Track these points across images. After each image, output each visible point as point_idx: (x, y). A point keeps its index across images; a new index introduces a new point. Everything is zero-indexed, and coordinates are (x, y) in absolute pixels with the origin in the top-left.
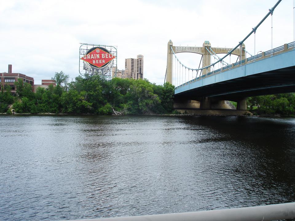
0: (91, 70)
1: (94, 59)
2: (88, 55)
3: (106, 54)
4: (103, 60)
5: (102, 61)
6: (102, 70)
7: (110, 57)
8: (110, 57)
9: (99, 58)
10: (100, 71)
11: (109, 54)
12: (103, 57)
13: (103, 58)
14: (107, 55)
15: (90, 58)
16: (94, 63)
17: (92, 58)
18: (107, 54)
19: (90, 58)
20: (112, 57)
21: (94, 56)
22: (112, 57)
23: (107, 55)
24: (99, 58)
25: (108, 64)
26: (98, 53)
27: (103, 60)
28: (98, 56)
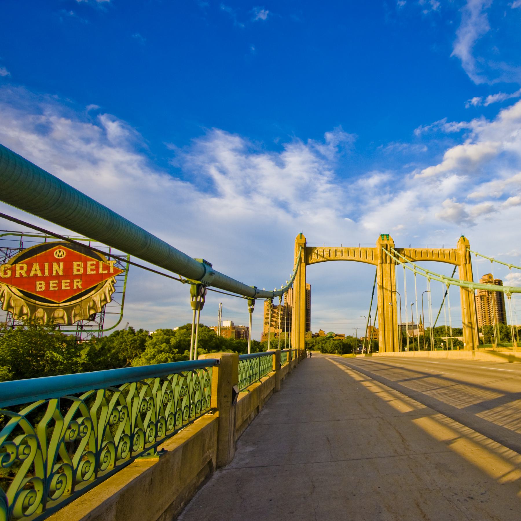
0: (26, 310)
1: (43, 278)
2: (18, 266)
3: (89, 263)
4: (75, 281)
5: (71, 284)
6: (68, 310)
7: (101, 271)
8: (101, 271)
9: (61, 273)
10: (60, 313)
11: (101, 263)
12: (78, 270)
13: (75, 272)
14: (92, 265)
15: (25, 275)
16: (38, 289)
17: (36, 275)
18: (95, 263)
19: (25, 275)
20: (112, 271)
21: (42, 270)
22: (112, 271)
23: (92, 265)
24: (61, 273)
25: (93, 292)
26: (58, 261)
27: (75, 281)
28: (58, 269)
